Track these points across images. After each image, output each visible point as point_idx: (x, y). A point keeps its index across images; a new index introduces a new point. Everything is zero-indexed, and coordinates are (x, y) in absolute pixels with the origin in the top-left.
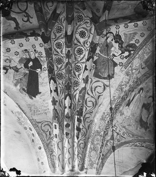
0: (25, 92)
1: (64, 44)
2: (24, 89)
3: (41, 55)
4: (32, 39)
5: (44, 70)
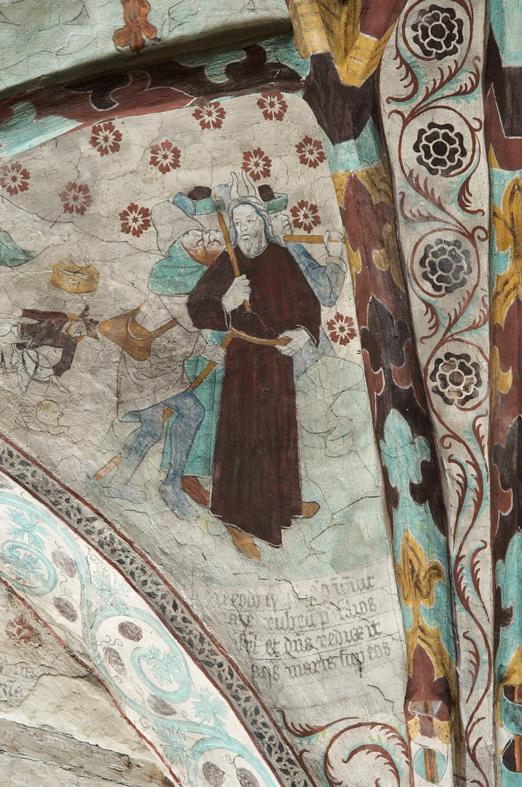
0: (202, 502)
1: (480, 135)
2: (191, 486)
3: (308, 229)
4: (240, 108)
5: (334, 337)
